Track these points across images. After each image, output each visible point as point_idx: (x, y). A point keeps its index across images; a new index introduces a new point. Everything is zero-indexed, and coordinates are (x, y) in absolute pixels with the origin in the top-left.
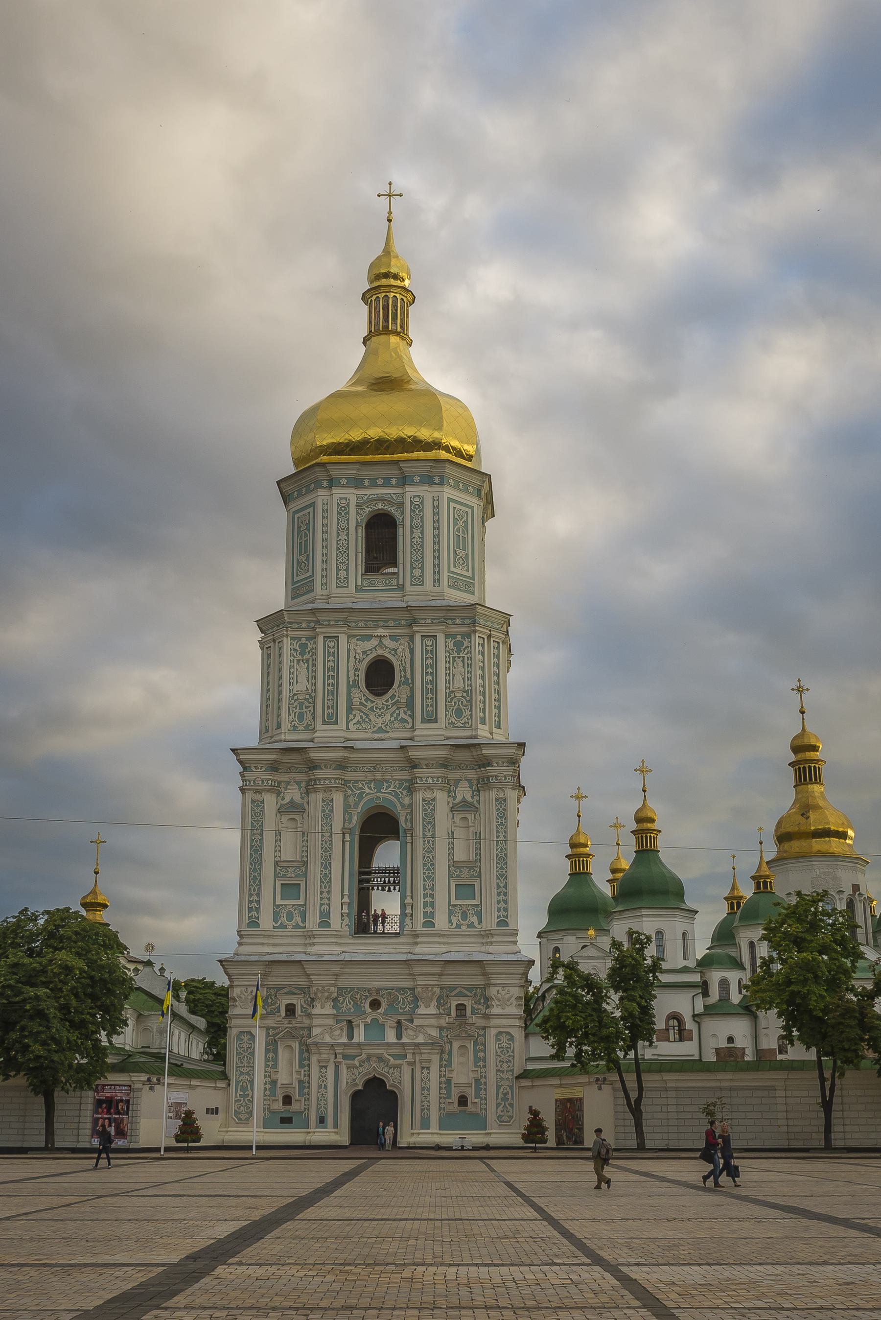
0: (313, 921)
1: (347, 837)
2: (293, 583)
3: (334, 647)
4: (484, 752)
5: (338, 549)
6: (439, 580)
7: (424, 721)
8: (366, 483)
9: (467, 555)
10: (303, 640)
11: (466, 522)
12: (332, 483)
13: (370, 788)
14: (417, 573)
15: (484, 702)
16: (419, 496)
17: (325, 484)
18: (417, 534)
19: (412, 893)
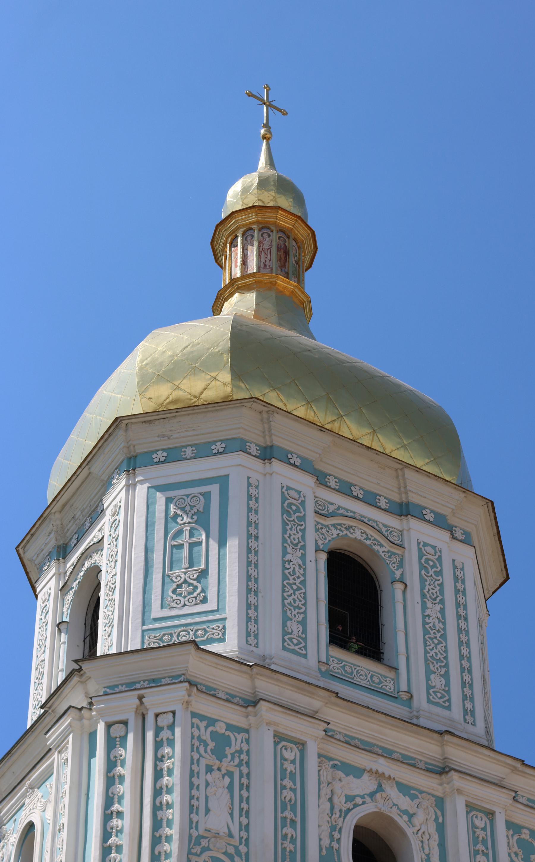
3: (293, 762)
5: (285, 577)
6: (473, 712)
10: (221, 728)
12: (267, 454)
17: (254, 450)
18: (433, 610)
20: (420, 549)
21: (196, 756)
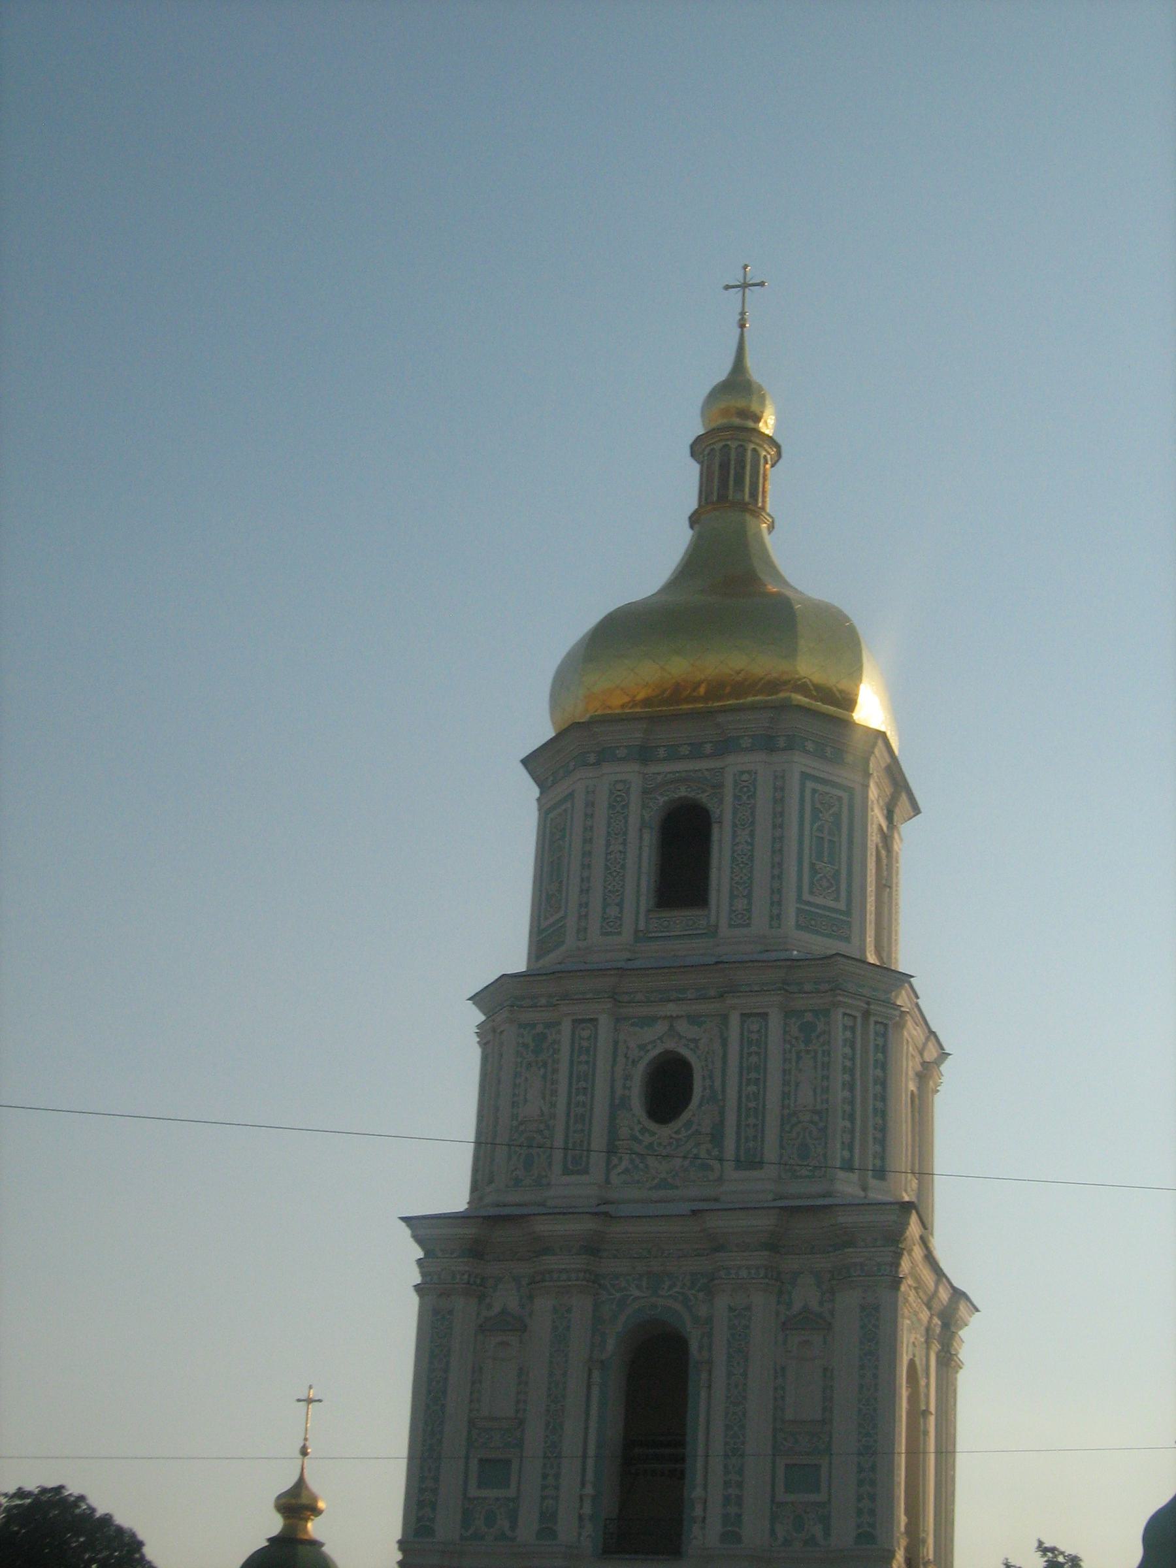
0: (528, 1528)
1: (596, 1374)
2: (540, 932)
3: (588, 1039)
4: (841, 1220)
5: (607, 868)
6: (779, 916)
7: (739, 1164)
8: (662, 752)
9: (838, 871)
10: (540, 1029)
11: (837, 816)
12: (605, 756)
13: (638, 1287)
14: (741, 904)
15: (852, 1131)
16: (749, 772)
17: (592, 758)
19: (705, 1477)
20: (735, 781)
21: (519, 1060)
